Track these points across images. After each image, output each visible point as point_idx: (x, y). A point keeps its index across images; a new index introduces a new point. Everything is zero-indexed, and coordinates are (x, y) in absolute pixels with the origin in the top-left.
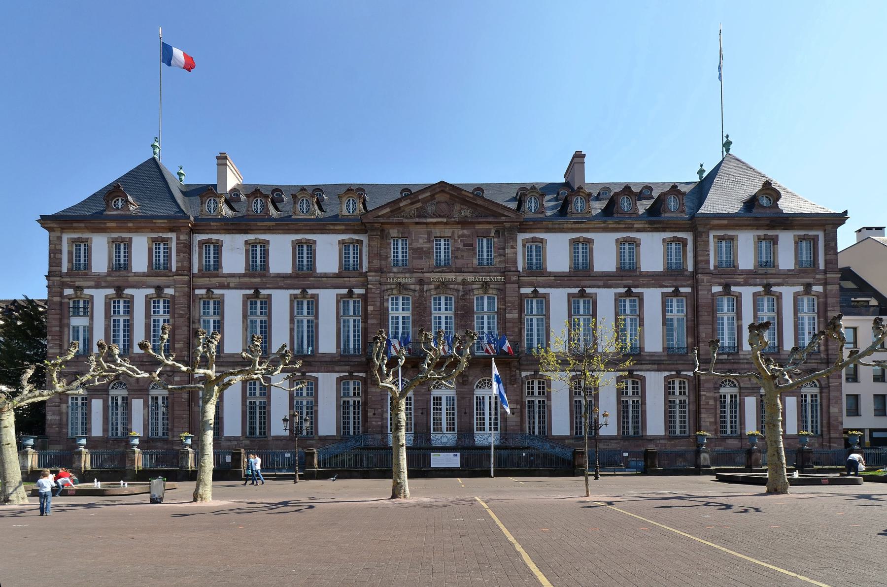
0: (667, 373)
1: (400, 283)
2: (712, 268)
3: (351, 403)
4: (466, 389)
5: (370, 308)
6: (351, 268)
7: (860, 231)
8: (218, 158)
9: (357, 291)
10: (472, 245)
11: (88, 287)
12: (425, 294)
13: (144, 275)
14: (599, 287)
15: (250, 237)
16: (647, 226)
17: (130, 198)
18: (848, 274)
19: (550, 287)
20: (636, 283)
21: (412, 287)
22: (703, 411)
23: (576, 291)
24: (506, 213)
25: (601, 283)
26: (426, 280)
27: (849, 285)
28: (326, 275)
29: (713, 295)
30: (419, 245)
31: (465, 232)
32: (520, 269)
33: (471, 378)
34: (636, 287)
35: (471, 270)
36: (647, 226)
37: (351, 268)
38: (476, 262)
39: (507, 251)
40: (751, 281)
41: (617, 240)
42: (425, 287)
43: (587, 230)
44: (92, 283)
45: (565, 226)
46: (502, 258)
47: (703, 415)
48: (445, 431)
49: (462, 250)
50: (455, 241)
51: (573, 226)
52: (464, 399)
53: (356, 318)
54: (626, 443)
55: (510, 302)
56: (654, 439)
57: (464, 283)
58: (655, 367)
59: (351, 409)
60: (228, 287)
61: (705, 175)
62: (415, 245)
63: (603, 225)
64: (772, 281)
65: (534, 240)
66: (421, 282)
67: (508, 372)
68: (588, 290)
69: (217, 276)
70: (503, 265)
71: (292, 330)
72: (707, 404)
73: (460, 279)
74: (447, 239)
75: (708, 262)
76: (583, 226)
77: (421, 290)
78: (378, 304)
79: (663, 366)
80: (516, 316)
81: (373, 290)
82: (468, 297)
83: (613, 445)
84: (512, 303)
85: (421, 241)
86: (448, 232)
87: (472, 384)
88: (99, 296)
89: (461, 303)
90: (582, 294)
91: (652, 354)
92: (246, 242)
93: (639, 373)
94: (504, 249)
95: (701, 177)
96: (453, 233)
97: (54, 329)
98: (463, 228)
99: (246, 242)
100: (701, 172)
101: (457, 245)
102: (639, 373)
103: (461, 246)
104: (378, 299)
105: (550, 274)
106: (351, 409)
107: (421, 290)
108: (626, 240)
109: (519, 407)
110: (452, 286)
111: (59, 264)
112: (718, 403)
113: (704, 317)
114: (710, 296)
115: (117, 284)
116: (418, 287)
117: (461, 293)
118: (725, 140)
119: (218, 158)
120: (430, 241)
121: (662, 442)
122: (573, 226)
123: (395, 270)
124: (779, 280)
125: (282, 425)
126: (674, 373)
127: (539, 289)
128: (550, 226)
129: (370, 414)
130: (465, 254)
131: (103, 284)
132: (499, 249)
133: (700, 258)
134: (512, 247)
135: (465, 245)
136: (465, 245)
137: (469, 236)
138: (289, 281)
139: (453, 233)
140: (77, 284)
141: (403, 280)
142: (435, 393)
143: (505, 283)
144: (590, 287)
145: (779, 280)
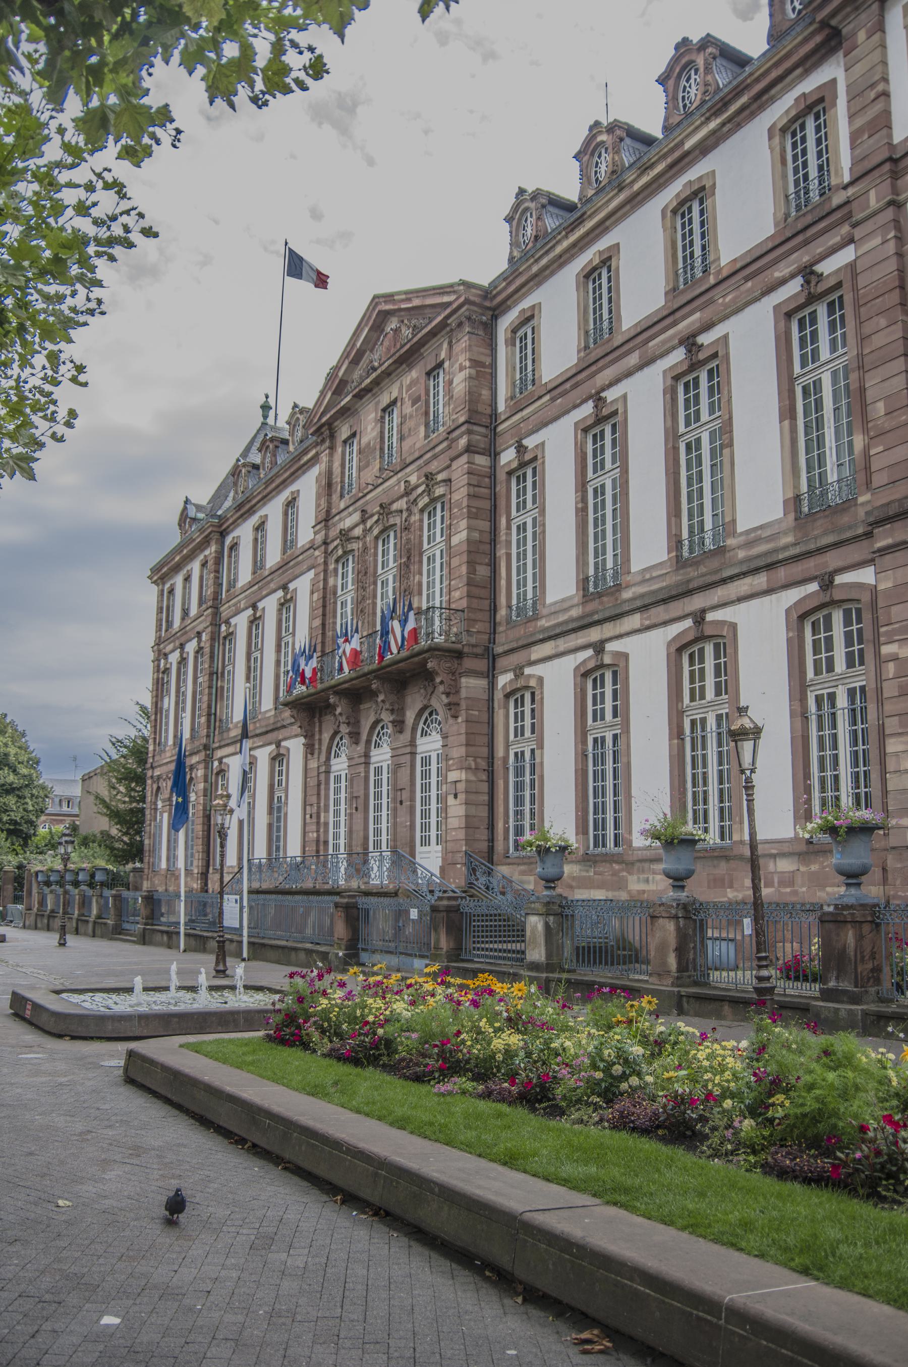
0: (793, 596)
14: (629, 374)
16: (713, 125)
22: (892, 725)
23: (587, 409)
25: (633, 359)
31: (414, 374)
34: (707, 327)
35: (417, 455)
36: (713, 125)
42: (369, 524)
45: (559, 249)
49: (411, 416)
51: (573, 238)
58: (761, 581)
63: (622, 197)
74: (394, 403)
76: (589, 224)
77: (367, 531)
79: (782, 574)
85: (369, 428)
91: (753, 537)
110: (395, 507)
122: (573, 238)
126: (813, 587)
144: (611, 385)
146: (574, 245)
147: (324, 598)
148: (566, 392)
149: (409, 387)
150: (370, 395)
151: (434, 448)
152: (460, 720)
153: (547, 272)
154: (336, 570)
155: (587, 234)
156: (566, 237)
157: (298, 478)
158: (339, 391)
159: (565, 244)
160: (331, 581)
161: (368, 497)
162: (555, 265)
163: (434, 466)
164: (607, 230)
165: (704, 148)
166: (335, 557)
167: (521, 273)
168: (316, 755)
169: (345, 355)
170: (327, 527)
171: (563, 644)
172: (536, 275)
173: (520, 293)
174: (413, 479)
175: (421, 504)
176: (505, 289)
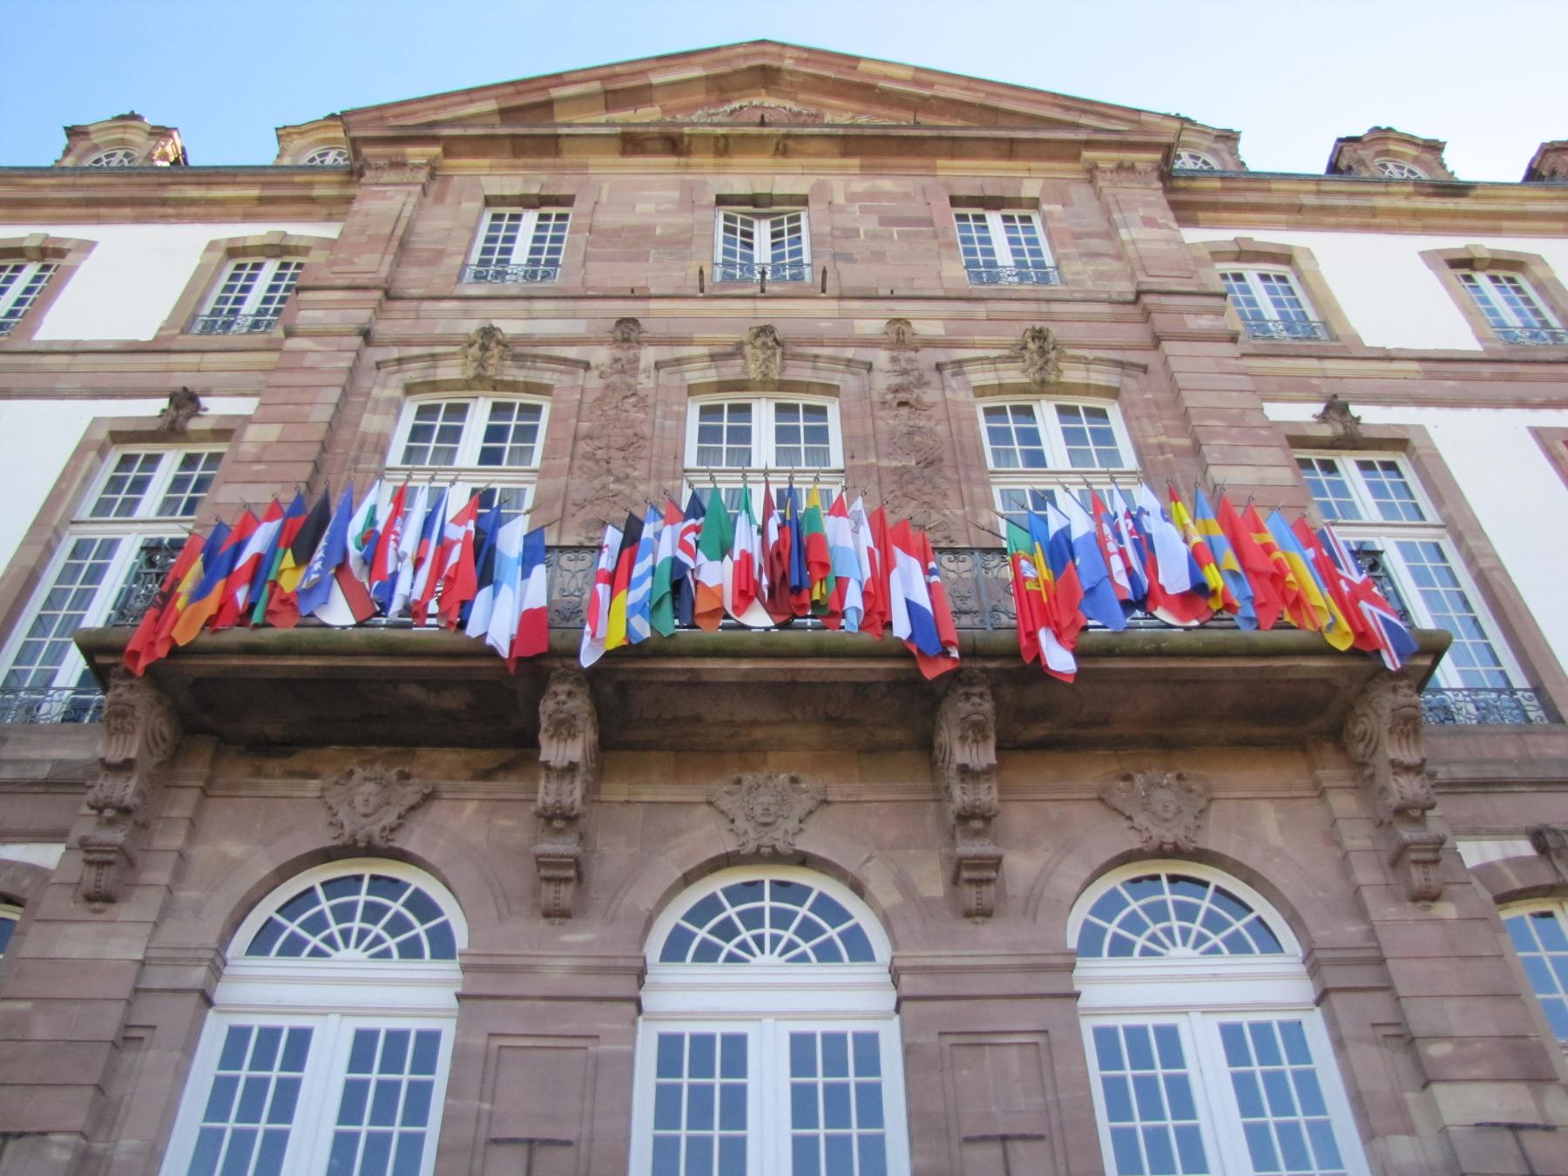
1: (488, 332)
4: (989, 944)
10: (930, 223)
12: (645, 383)
24: (1084, 120)
26: (651, 327)
28: (75, 350)
30: (630, 220)
31: (886, 184)
33: (1020, 866)
35: (941, 293)
38: (955, 272)
39: (1124, 234)
42: (649, 355)
43: (1493, 222)
45: (1381, 202)
46: (1108, 265)
49: (872, 236)
52: (976, 1041)
62: (606, 219)
65: (1246, 254)
66: (628, 332)
67: (1344, 803)
70: (1125, 288)
73: (871, 325)
78: (322, 413)
81: (309, 361)
82: (930, 395)
86: (786, 180)
87: (1041, 904)
89: (891, 421)
94: (1110, 233)
96: (821, 187)
98: (865, 170)
101: (840, 220)
104: (334, 395)
107: (627, 368)
116: (601, 355)
117: (882, 382)
120: (689, 203)
127: (1355, 410)
128: (1309, 200)
132: (1077, 236)
137: (906, 196)
139: (821, 187)
141: (509, 328)
142: (687, 997)
143: (1157, 341)
146: (1415, 214)
147: (325, 446)
148: (1477, 378)
149: (852, 198)
150: (673, 160)
151: (1048, 301)
152: (1446, 910)
153: (1332, 220)
154: (398, 407)
155: (1454, 214)
156: (1408, 196)
157: (99, 220)
158: (506, 114)
159: (1402, 204)
160: (371, 423)
161: (654, 304)
162: (1356, 220)
164: (1496, 231)
166: (414, 373)
167: (1269, 190)
168: (137, 910)
169: (606, 74)
170: (379, 311)
172: (1300, 209)
173: (1242, 216)
175: (978, 377)
176: (1214, 191)
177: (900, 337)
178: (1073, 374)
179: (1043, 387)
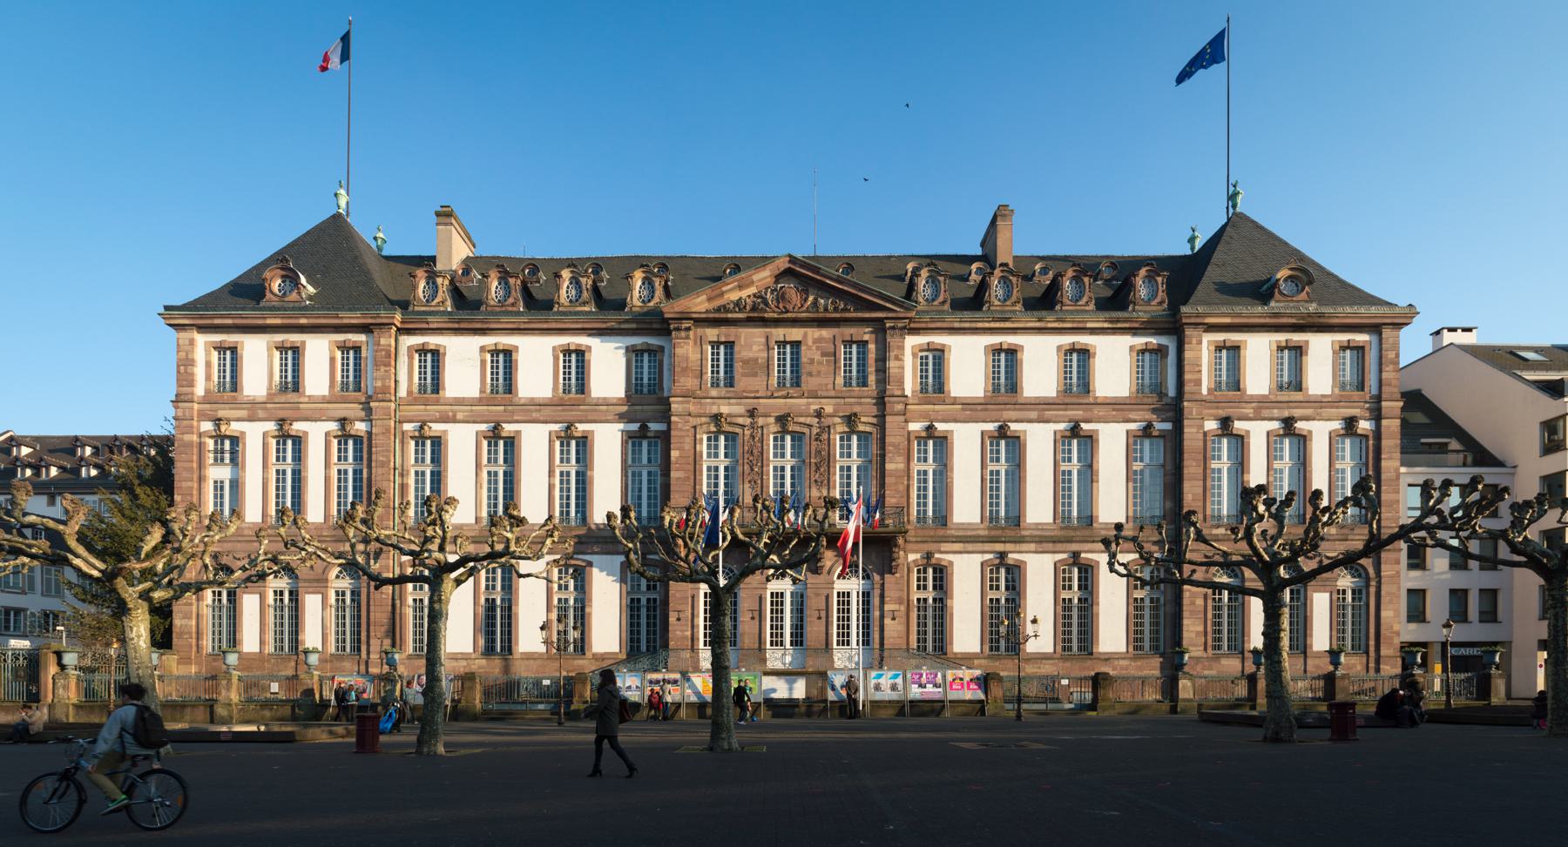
2: (1205, 391)
3: (644, 601)
5: (674, 454)
6: (645, 390)
7: (1438, 333)
8: (438, 214)
9: (654, 426)
11: (238, 420)
13: (324, 400)
15: (489, 341)
17: (303, 280)
18: (1414, 400)
19: (956, 421)
20: (1088, 415)
21: (740, 420)
22: (1185, 614)
25: (1034, 415)
26: (761, 410)
27: (1419, 418)
29: (1205, 434)
30: (751, 355)
32: (908, 392)
34: (1087, 421)
35: (832, 393)
37: (645, 390)
40: (1265, 413)
41: (1059, 348)
42: (761, 421)
44: (243, 413)
45: (980, 325)
47: (1185, 622)
48: (788, 645)
49: (820, 363)
50: (809, 348)
51: (993, 325)
53: (652, 469)
54: (1068, 664)
55: (893, 445)
56: (1108, 658)
57: (819, 414)
59: (644, 612)
60: (454, 421)
61: (1198, 244)
63: (1038, 325)
64: (1297, 413)
66: (752, 413)
68: (1014, 426)
69: (437, 403)
71: (551, 487)
72: (1193, 603)
75: (1198, 382)
77: (752, 426)
80: (902, 466)
83: (1047, 669)
84: (896, 446)
85: (755, 348)
88: (255, 434)
90: (1002, 432)
92: (482, 349)
93: (1089, 556)
95: (1192, 248)
96: (805, 335)
97: (184, 484)
99: (482, 349)
100: (1192, 240)
102: (1089, 556)
103: (817, 357)
105: (955, 401)
106: (644, 612)
108: (1072, 350)
109: (903, 608)
110: (802, 420)
111: (191, 384)
112: (1210, 602)
113: (1191, 468)
114: (1201, 436)
115: (282, 414)
116: (748, 421)
117: (815, 431)
118: (1231, 189)
119: (438, 214)
121: (1122, 662)
123: (714, 393)
124: (1308, 412)
125: (539, 636)
128: (957, 325)
129: (672, 619)
130: (823, 369)
131: (261, 414)
133: (1187, 376)
134: (897, 358)
135: (823, 355)
136: (823, 355)
138: (547, 411)
139: (805, 335)
140: (221, 414)
141: (725, 410)
145: (1308, 412)
163: (857, 409)
165: (1093, 331)
171: (979, 546)
174: (829, 409)
177: (819, 414)
178: (861, 428)
179: (853, 432)
